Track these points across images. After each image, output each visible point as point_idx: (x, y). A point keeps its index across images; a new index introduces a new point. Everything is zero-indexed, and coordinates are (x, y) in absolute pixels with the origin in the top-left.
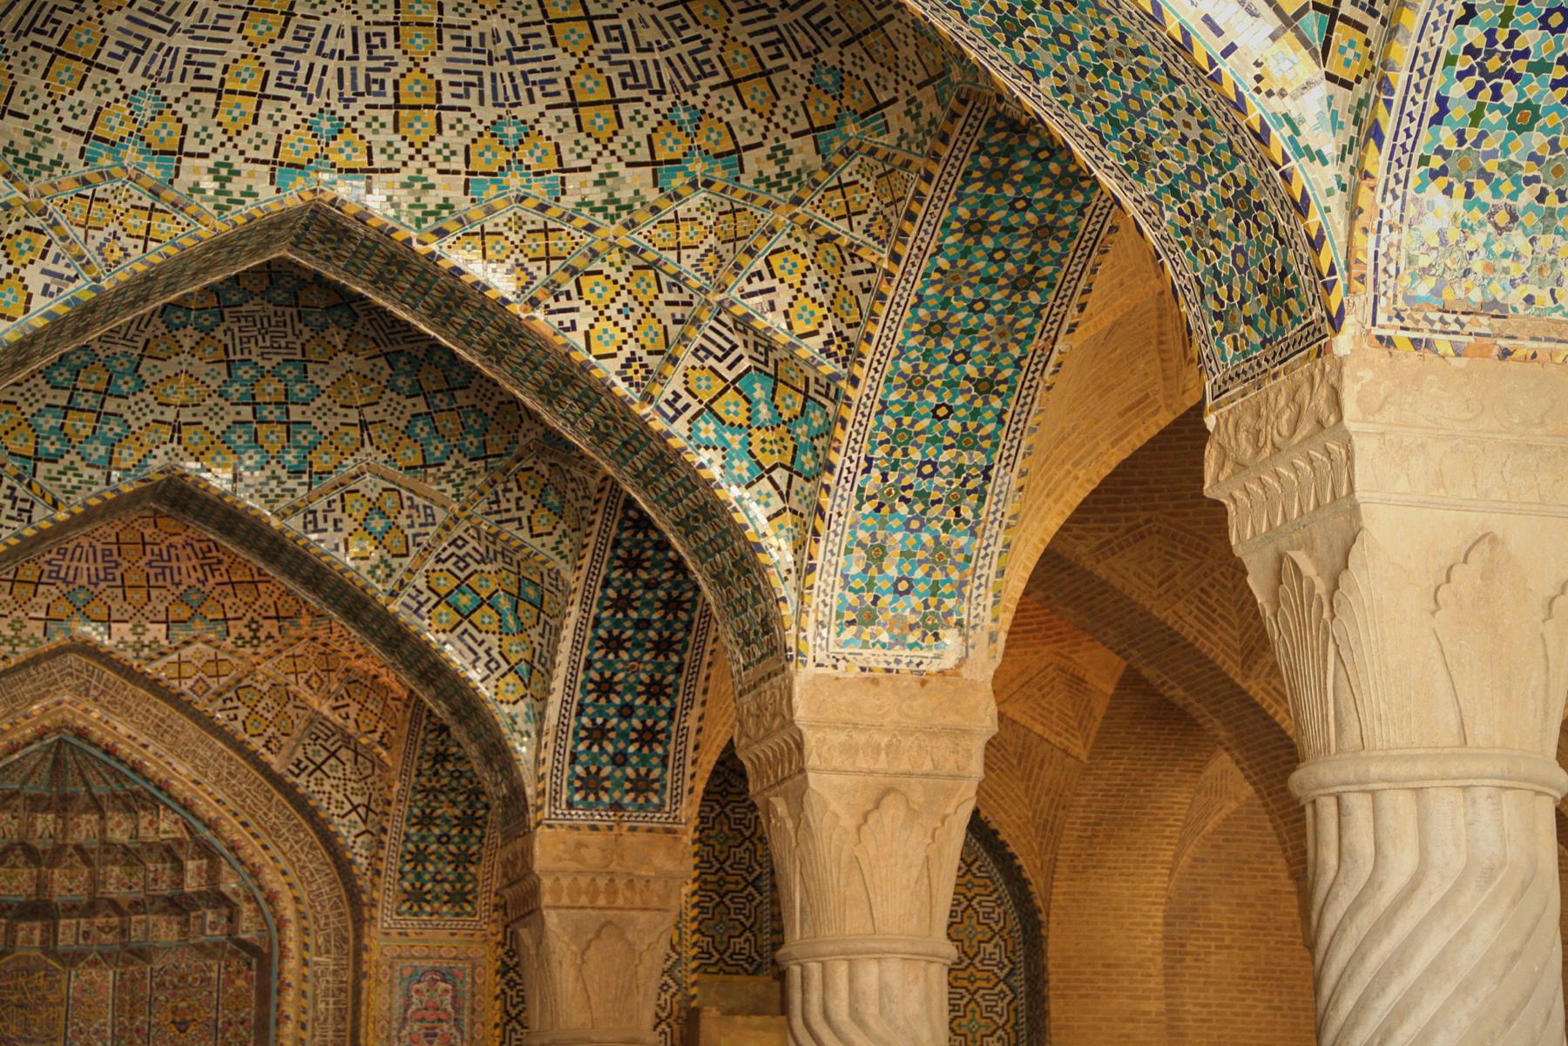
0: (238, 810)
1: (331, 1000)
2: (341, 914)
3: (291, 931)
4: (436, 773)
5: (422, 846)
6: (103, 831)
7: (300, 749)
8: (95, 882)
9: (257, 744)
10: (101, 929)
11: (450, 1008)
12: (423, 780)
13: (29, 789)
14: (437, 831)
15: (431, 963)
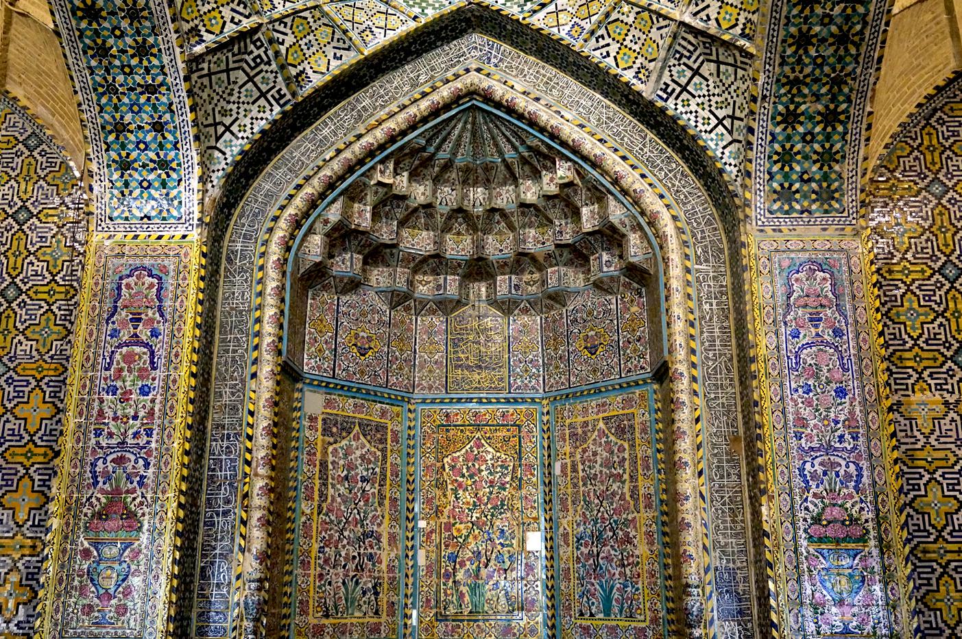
0: (618, 147)
1: (714, 302)
2: (715, 229)
3: (673, 244)
4: (800, 61)
5: (788, 146)
6: (518, 196)
7: (667, 73)
8: (519, 241)
9: (628, 76)
10: (527, 283)
11: (830, 295)
12: (787, 69)
13: (460, 161)
14: (801, 129)
15: (807, 255)
